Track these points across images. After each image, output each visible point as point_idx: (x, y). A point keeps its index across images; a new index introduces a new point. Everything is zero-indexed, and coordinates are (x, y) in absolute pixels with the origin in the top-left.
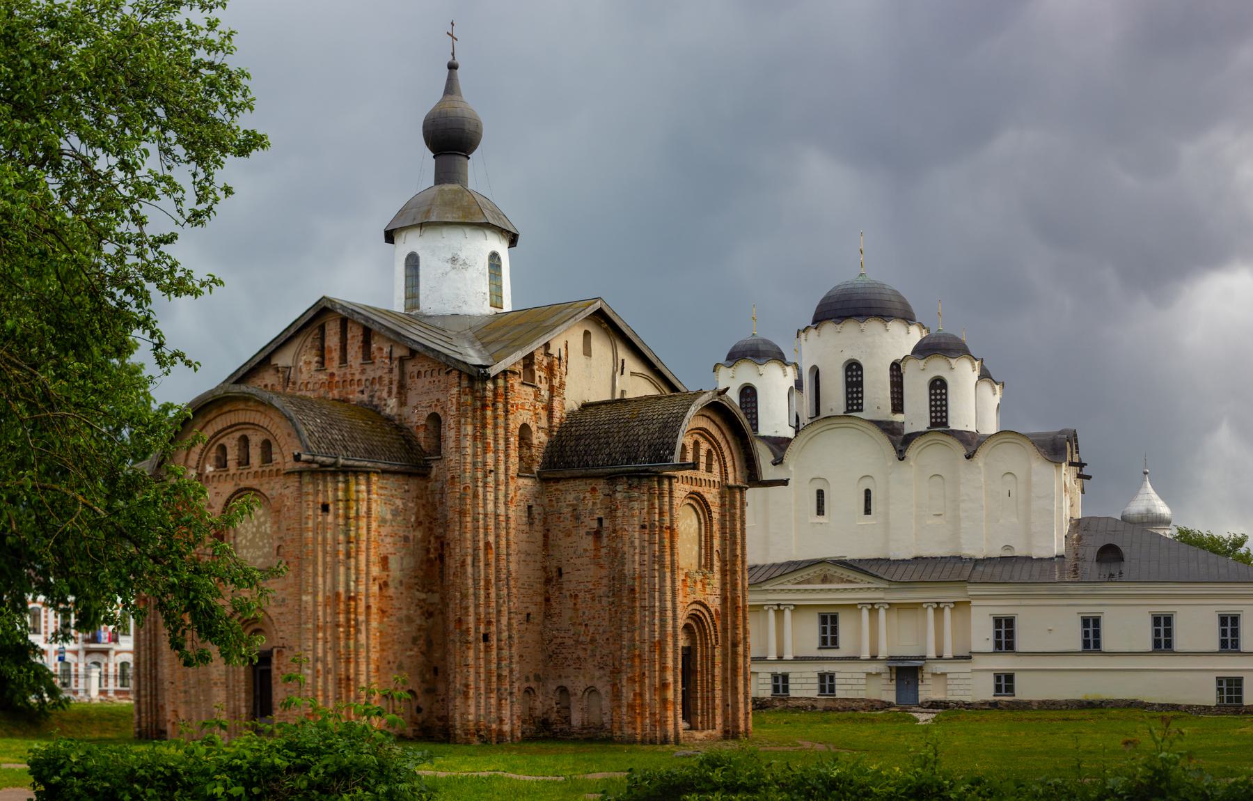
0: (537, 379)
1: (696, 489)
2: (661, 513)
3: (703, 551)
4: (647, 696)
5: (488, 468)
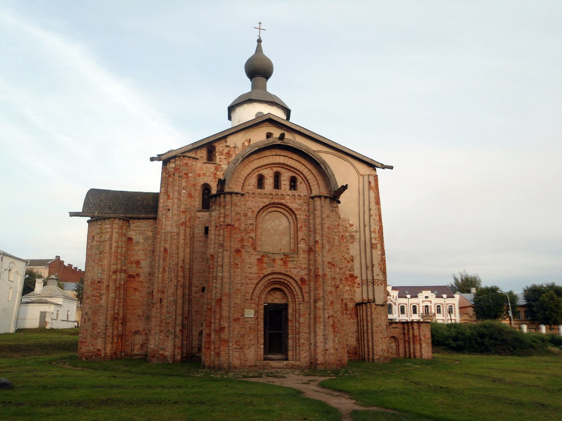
0: (218, 160)
1: (276, 201)
2: (225, 217)
3: (292, 241)
4: (213, 336)
5: (168, 208)
